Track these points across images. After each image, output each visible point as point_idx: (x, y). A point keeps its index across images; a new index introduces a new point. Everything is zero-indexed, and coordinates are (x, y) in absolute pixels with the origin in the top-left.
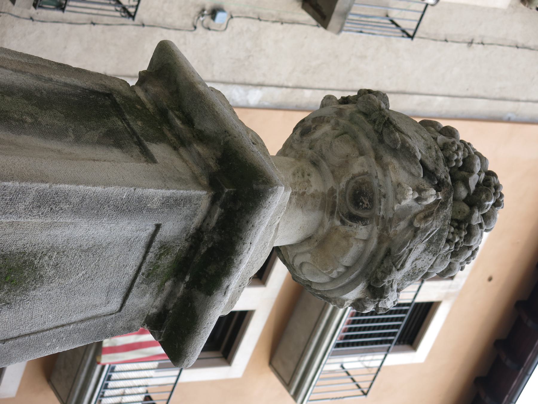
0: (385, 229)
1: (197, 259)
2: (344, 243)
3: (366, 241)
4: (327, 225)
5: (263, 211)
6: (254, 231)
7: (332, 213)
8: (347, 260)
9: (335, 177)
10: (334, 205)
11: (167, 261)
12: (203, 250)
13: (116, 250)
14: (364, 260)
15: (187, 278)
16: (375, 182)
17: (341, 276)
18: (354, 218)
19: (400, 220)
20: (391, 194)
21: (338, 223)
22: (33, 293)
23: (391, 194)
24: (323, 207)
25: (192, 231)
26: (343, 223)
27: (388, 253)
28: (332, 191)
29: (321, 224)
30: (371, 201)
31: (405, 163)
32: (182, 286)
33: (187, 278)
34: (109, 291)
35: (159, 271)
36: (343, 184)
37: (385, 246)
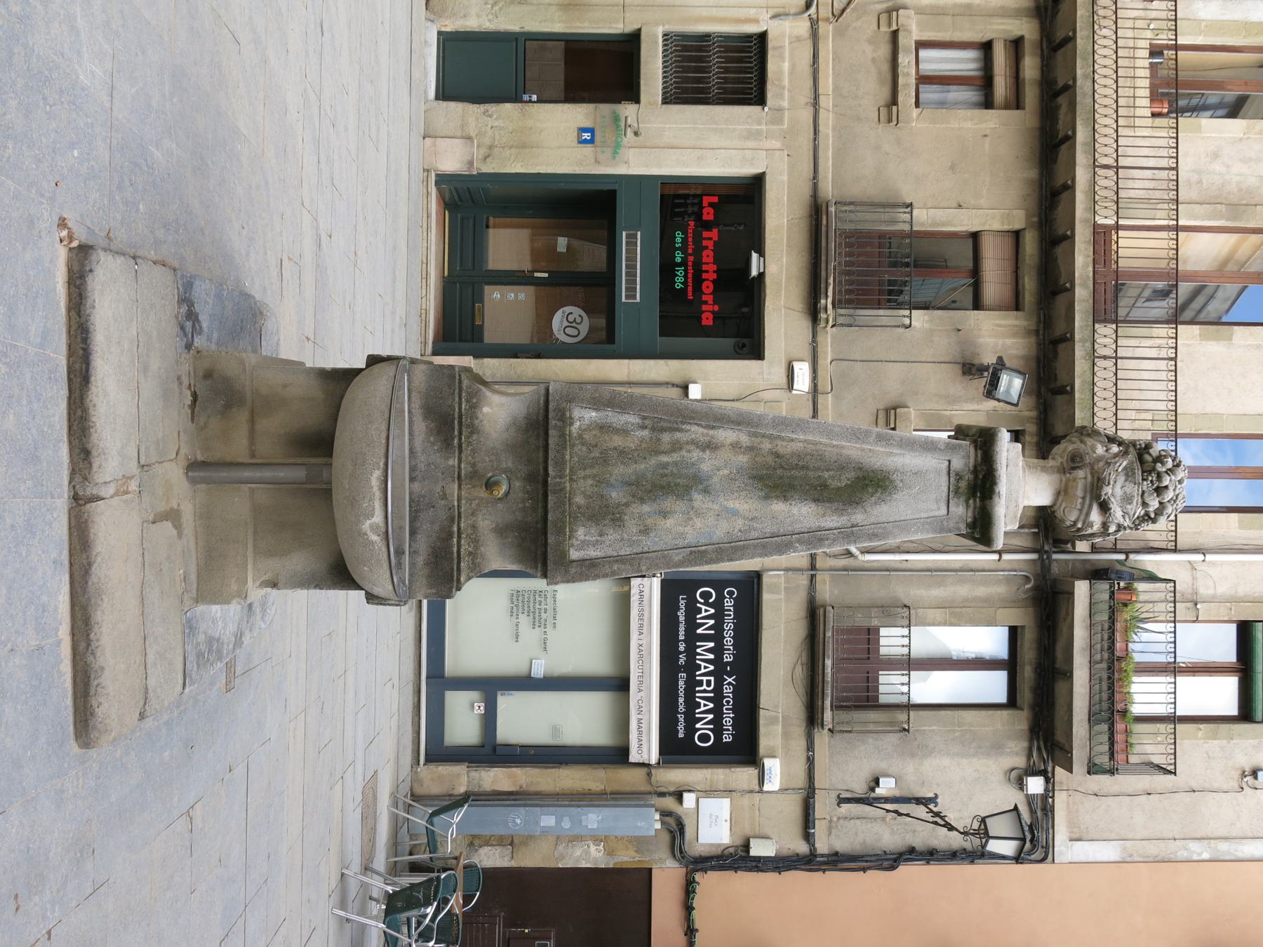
0: (1092, 468)
1: (979, 482)
2: (1074, 484)
3: (1085, 478)
4: (1064, 479)
5: (999, 443)
6: (998, 456)
7: (1064, 473)
8: (1080, 493)
9: (1061, 457)
10: (1064, 468)
11: (963, 484)
12: (981, 477)
13: (932, 475)
14: (1088, 489)
15: (978, 495)
16: (1081, 451)
17: (1083, 504)
18: (1074, 468)
19: (1099, 461)
20: (1090, 452)
21: (1068, 475)
22: (895, 496)
23: (1090, 452)
24: (1058, 471)
25: (972, 468)
26: (1070, 473)
27: (1099, 479)
28: (1062, 463)
29: (1061, 481)
30: (1081, 458)
31: (1095, 438)
32: (978, 500)
33: (978, 495)
34: (937, 501)
35: (961, 490)
36: (1065, 458)
37: (1095, 477)
